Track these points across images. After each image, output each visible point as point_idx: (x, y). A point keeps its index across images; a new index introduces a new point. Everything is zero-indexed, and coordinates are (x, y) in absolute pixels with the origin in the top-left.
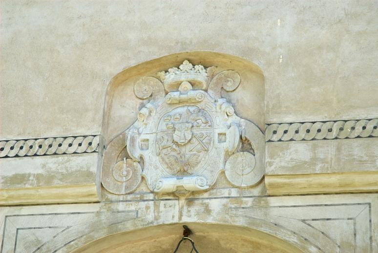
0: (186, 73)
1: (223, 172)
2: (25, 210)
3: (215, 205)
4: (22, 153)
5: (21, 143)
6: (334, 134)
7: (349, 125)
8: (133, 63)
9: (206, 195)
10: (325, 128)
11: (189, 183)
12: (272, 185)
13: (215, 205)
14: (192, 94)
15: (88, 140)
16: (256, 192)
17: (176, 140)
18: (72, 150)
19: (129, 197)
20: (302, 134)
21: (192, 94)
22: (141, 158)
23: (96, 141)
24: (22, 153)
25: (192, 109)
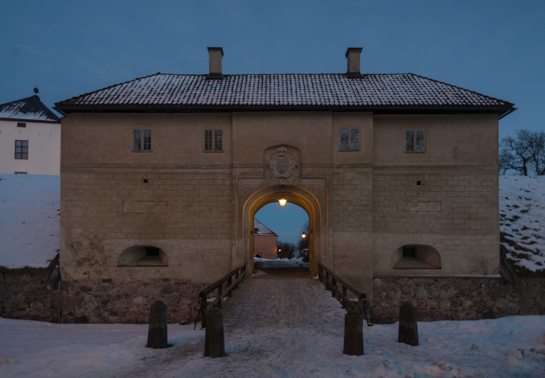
0: (282, 149)
1: (291, 173)
2: (246, 180)
3: (290, 180)
4: (244, 167)
5: (244, 165)
6: (316, 166)
7: (320, 164)
8: (270, 146)
9: (288, 178)
10: (315, 165)
11: (284, 175)
12: (303, 177)
13: (290, 180)
14: (284, 154)
15: (260, 164)
16: (299, 178)
17: (281, 165)
18: (256, 167)
19: (270, 178)
20: (310, 166)
21: (284, 154)
22: (272, 169)
23: (262, 165)
24: (244, 167)
25: (284, 158)
